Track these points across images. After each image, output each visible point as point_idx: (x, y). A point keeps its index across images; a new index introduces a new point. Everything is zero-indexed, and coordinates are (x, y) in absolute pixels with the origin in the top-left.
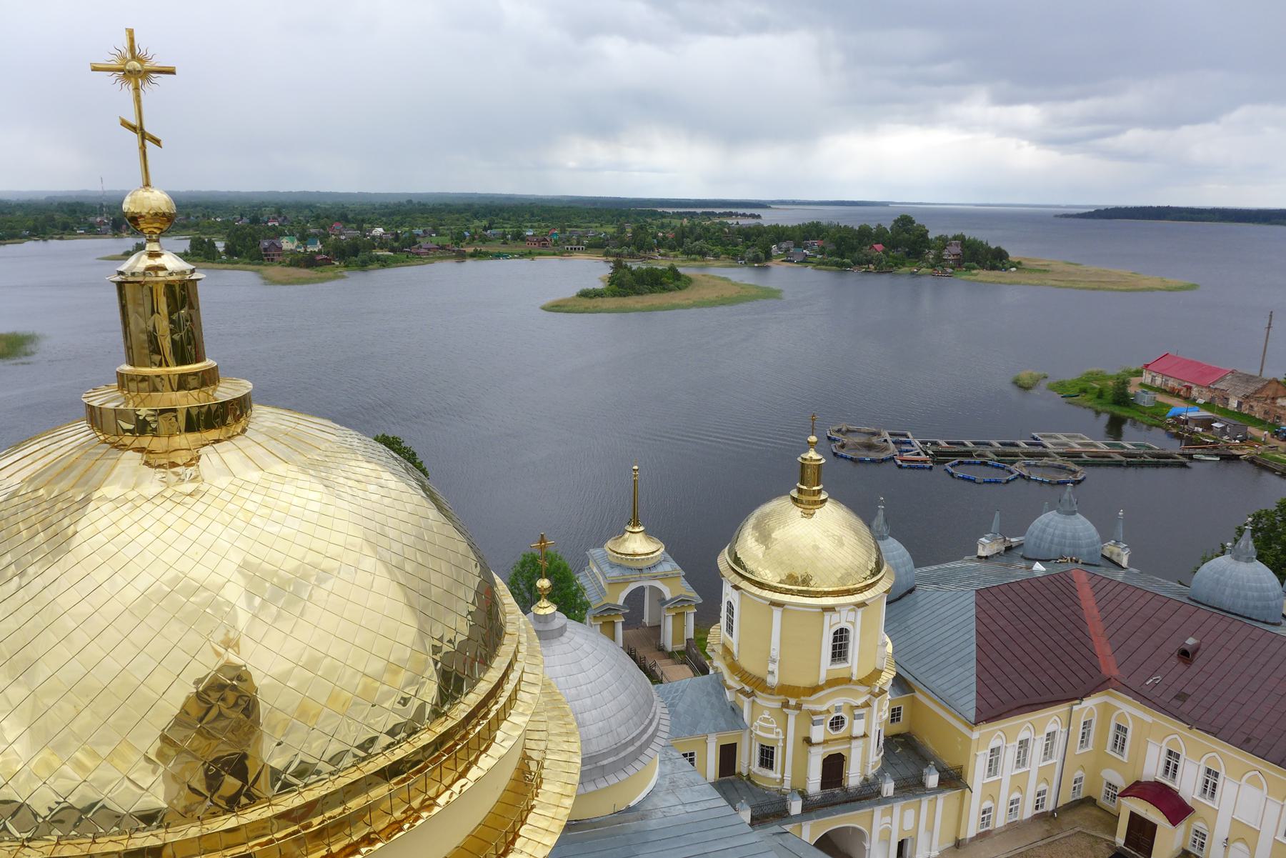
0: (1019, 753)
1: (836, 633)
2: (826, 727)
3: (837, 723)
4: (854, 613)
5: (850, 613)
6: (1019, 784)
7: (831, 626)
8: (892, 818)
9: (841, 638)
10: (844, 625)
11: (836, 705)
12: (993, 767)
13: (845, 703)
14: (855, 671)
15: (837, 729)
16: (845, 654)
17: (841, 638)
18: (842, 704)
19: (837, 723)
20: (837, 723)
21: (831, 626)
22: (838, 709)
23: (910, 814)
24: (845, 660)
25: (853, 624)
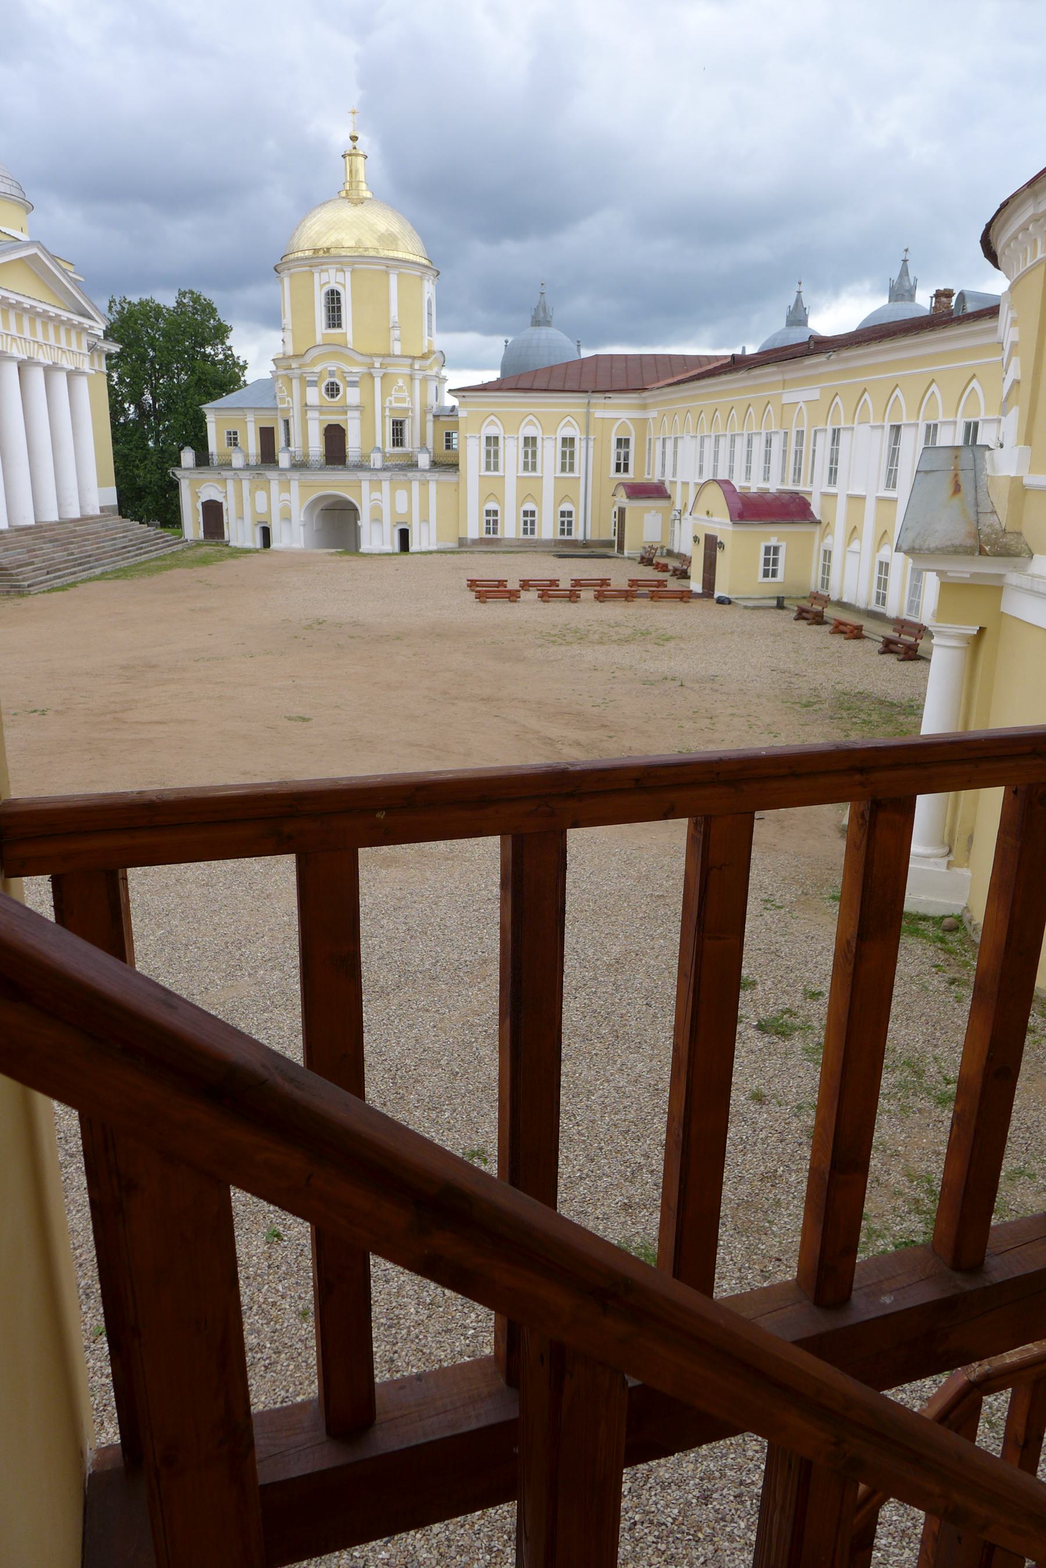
0: (526, 453)
1: (327, 294)
2: (320, 392)
3: (333, 390)
4: (343, 273)
5: (338, 273)
6: (529, 490)
7: (322, 286)
8: (381, 493)
9: (333, 299)
10: (333, 285)
11: (329, 369)
12: (492, 459)
13: (338, 368)
14: (350, 337)
15: (333, 396)
16: (339, 317)
17: (333, 299)
18: (335, 369)
19: (332, 390)
20: (333, 390)
21: (322, 286)
22: (332, 374)
23: (401, 495)
24: (340, 326)
25: (344, 286)
